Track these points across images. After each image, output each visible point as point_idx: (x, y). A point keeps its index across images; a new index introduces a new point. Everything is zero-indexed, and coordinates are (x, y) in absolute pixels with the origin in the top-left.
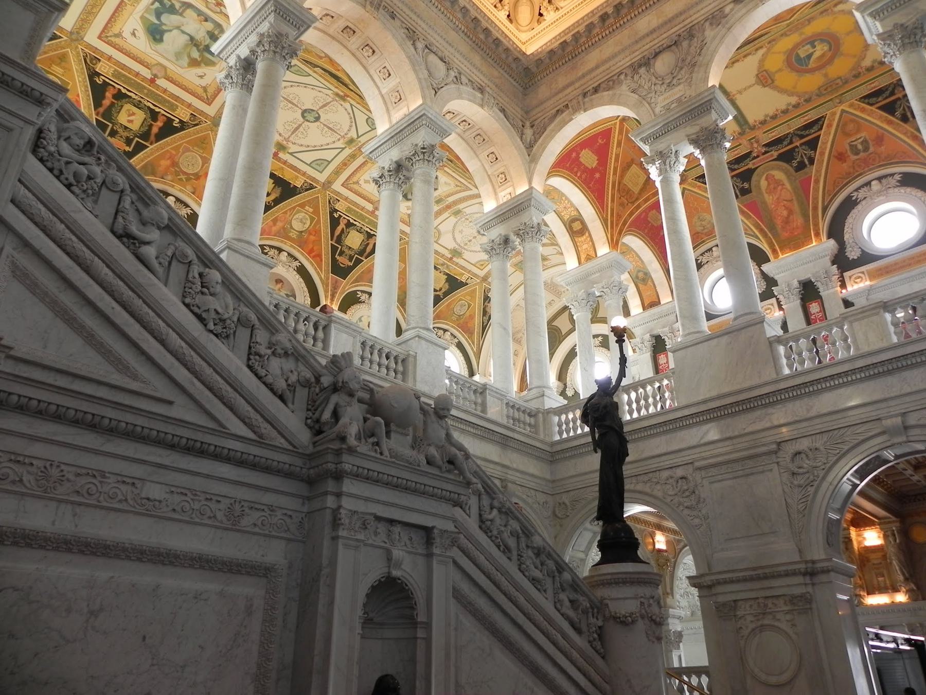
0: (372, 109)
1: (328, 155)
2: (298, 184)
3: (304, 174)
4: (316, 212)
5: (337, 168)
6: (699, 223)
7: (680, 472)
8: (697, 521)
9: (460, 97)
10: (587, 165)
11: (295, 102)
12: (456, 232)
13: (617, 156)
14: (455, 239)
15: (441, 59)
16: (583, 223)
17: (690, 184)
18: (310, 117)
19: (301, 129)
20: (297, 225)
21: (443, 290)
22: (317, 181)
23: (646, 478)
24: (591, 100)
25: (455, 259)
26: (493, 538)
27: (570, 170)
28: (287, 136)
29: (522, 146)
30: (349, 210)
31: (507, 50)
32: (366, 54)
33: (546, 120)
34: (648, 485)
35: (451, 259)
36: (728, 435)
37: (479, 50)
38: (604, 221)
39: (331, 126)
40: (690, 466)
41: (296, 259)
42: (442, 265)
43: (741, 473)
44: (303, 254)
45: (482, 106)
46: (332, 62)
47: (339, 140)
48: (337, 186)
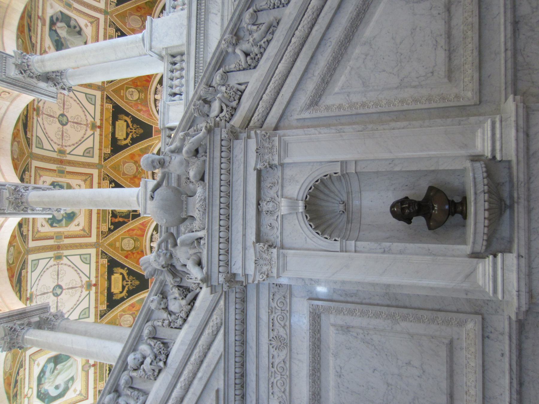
0: (26, 105)
1: (82, 97)
2: (110, 106)
3: (102, 105)
11: (60, 133)
18: (64, 120)
19: (75, 121)
20: (136, 96)
22: (102, 96)
26: (262, 50)
28: (85, 127)
39: (62, 105)
41: (156, 88)
44: (152, 85)
46: (15, 136)
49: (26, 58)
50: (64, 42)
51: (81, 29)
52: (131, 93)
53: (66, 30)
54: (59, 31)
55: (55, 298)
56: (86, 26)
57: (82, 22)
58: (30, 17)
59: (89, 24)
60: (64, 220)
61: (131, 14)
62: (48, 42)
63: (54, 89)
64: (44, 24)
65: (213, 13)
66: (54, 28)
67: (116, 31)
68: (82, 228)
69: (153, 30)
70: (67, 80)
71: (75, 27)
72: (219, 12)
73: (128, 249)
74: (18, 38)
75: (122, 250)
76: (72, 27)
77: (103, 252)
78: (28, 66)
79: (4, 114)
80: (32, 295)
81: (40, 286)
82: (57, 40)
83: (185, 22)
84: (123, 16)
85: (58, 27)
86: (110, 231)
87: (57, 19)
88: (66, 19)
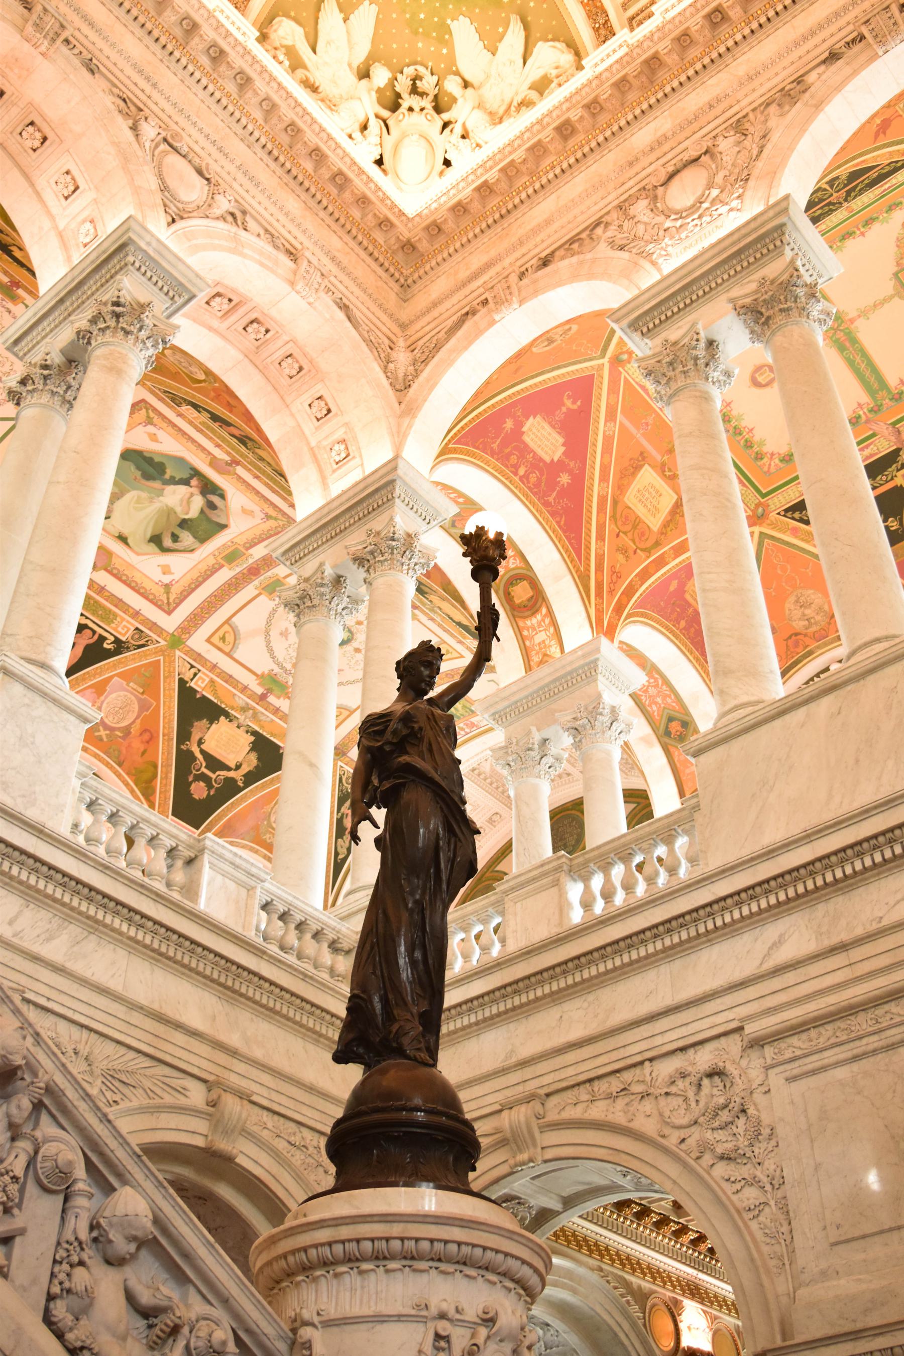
6: (797, 613)
7: (704, 1058)
8: (751, 1195)
9: (237, 249)
10: (540, 452)
12: (274, 633)
13: (608, 440)
14: (270, 650)
15: (200, 172)
16: (534, 584)
17: (774, 526)
21: (245, 769)
23: (615, 1084)
24: (535, 282)
25: (271, 699)
27: (504, 458)
29: (385, 382)
31: (363, 201)
32: (29, 144)
33: (443, 332)
34: (621, 1103)
35: (263, 697)
36: (835, 940)
37: (299, 190)
38: (582, 581)
40: (736, 1037)
42: (244, 709)
43: (873, 1042)
45: (292, 284)
49: (149, 344)
50: (152, 484)
51: (165, 550)
53: (178, 510)
54: (182, 489)
56: (166, 570)
57: (181, 565)
58: (244, 440)
59: (166, 579)
61: (143, 707)
62: (166, 445)
63: (37, 357)
64: (214, 463)
65: (20, 913)
66: (194, 482)
67: (117, 641)
69: (55, 709)
70: (43, 406)
71: (175, 538)
72: (15, 935)
74: (208, 372)
76: (178, 531)
78: (127, 333)
79: (38, 194)
82: (164, 472)
83: (32, 814)
84: (149, 683)
85: (192, 495)
87: (212, 506)
88: (205, 526)
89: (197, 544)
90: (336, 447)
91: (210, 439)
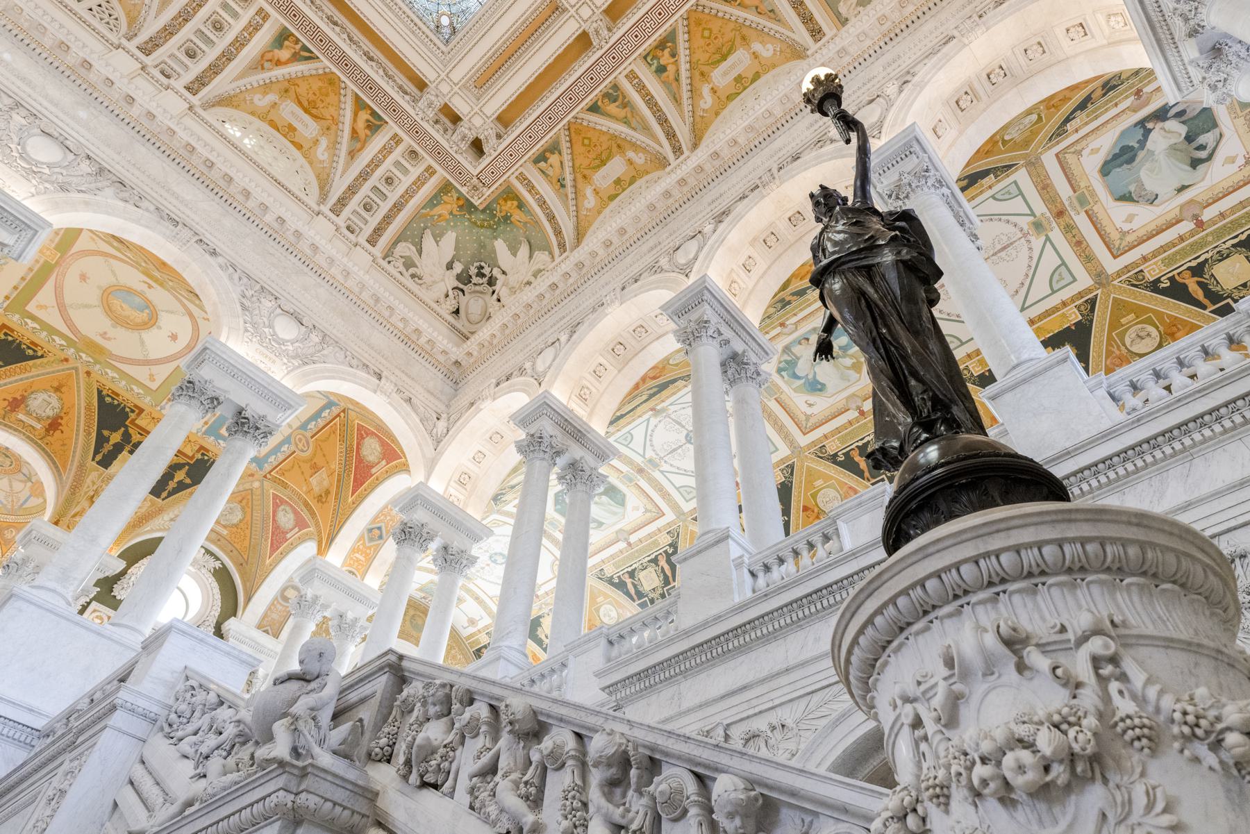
3: (1064, 304)
4: (1139, 311)
5: (1079, 256)
22: (1089, 290)
30: (1169, 261)
47: (1029, 241)
48: (1112, 266)
50: (1138, 159)
52: (1141, 334)
53: (1173, 141)
54: (1152, 136)
55: (684, 441)
56: (1232, 160)
60: (802, 381)
62: (1106, 143)
64: (1135, 110)
66: (1150, 125)
68: (809, 413)
69: (1041, 378)
71: (1201, 147)
73: (821, 505)
74: (1029, 112)
75: (814, 496)
76: (1195, 144)
77: (792, 467)
80: (663, 410)
81: (682, 412)
82: (1132, 148)
85: (1163, 129)
86: (833, 459)
89: (1217, 131)
90: (1112, 24)
91: (1107, 110)
